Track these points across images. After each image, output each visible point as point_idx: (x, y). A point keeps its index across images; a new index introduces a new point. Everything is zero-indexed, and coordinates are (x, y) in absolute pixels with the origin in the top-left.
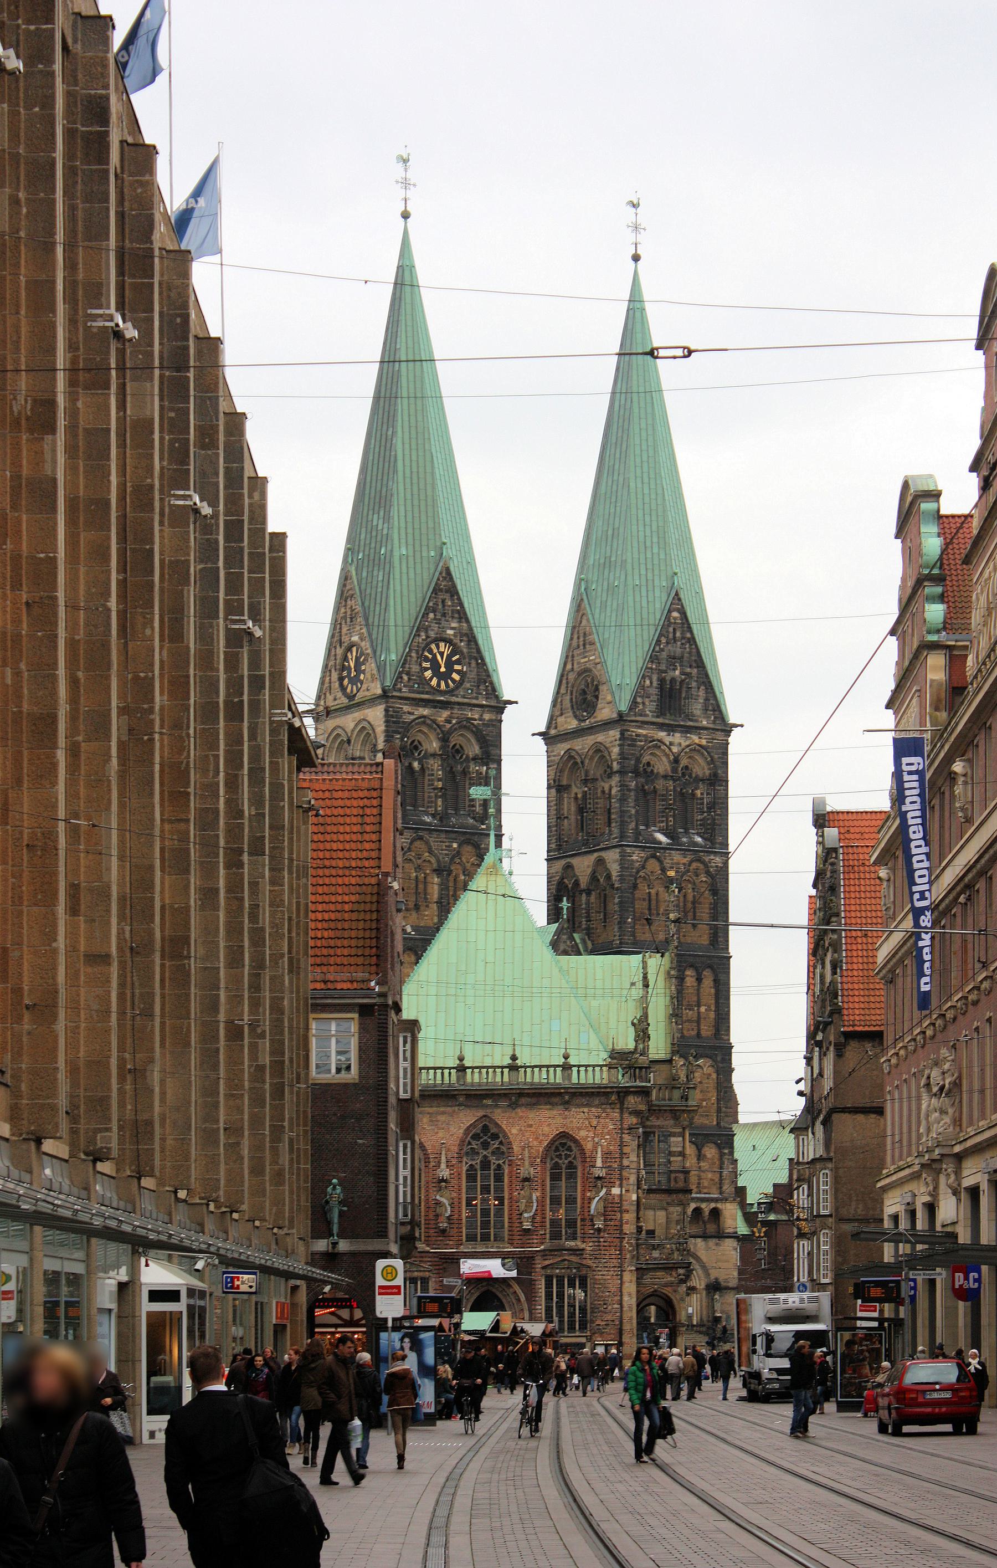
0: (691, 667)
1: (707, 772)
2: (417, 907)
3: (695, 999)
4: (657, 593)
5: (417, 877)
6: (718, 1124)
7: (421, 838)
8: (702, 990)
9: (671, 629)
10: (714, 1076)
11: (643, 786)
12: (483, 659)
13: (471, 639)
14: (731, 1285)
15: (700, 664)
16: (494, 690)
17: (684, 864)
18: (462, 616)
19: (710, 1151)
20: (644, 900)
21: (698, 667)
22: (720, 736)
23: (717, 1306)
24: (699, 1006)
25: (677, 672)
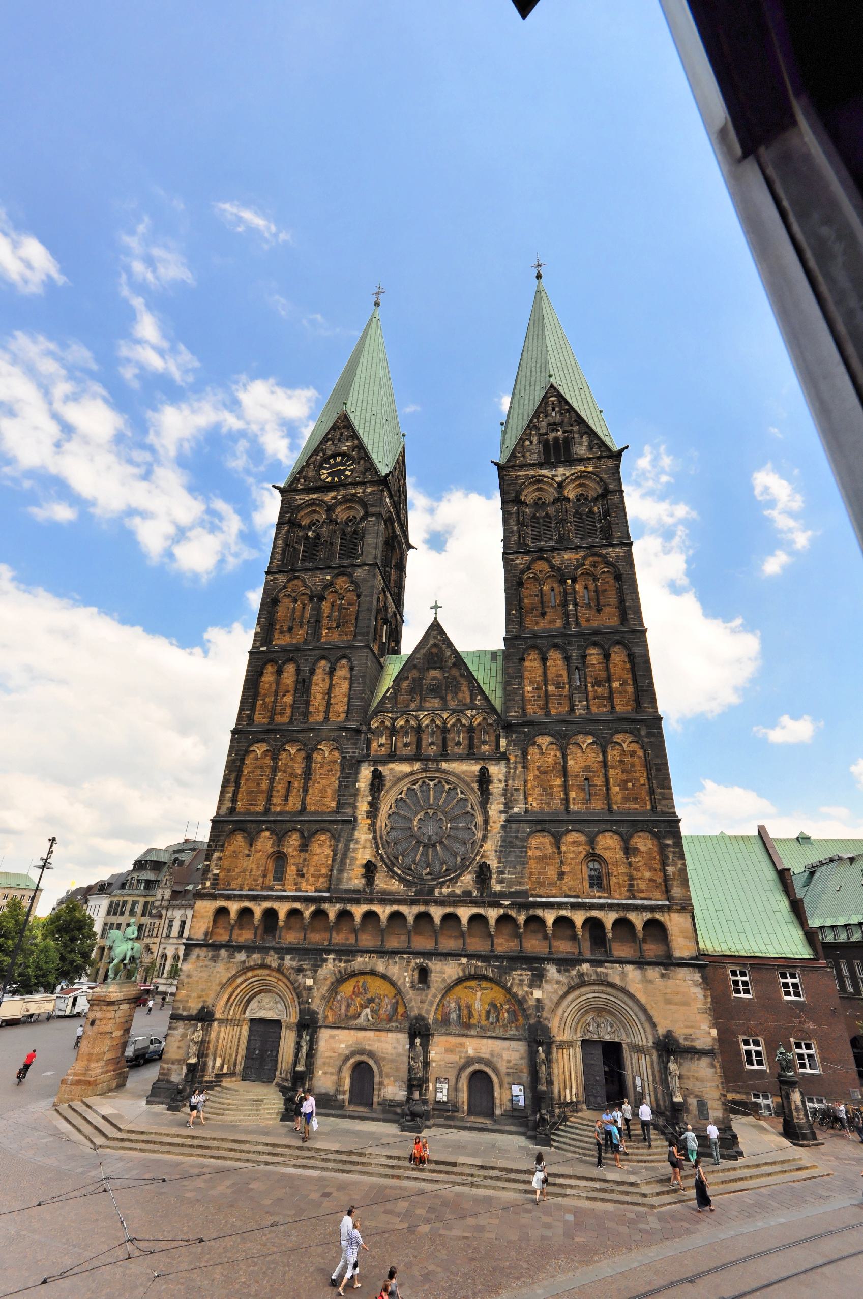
0: (572, 425)
1: (600, 491)
2: (290, 629)
3: (605, 675)
4: (537, 393)
5: (294, 608)
6: (654, 808)
7: (297, 577)
8: (612, 665)
9: (550, 408)
10: (640, 753)
11: (534, 515)
12: (368, 457)
13: (361, 447)
14: (699, 1044)
15: (580, 420)
16: (376, 472)
17: (577, 559)
18: (355, 436)
19: (643, 843)
20: (536, 596)
21: (579, 424)
22: (609, 463)
23: (675, 1083)
24: (609, 680)
25: (559, 433)
